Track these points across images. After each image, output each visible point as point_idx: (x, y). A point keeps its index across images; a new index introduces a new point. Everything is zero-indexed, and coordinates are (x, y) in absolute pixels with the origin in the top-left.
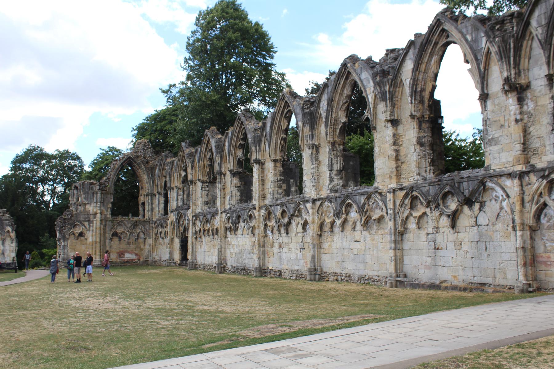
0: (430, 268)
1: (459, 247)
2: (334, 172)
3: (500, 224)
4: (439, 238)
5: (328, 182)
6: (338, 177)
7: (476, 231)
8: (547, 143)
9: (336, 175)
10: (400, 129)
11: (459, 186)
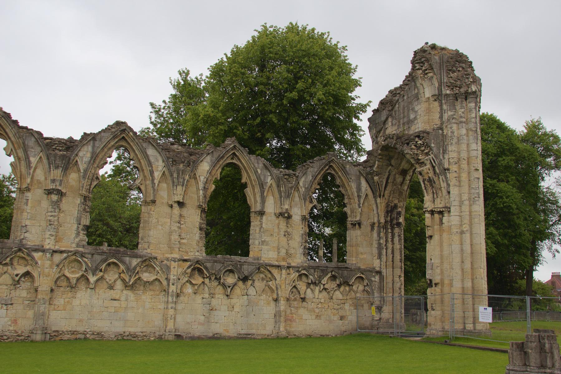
0: (202, 324)
1: (231, 309)
2: (81, 227)
3: (264, 296)
4: (214, 302)
5: (74, 235)
6: (85, 232)
7: (246, 299)
8: (298, 252)
9: (83, 230)
10: (185, 211)
11: (241, 267)
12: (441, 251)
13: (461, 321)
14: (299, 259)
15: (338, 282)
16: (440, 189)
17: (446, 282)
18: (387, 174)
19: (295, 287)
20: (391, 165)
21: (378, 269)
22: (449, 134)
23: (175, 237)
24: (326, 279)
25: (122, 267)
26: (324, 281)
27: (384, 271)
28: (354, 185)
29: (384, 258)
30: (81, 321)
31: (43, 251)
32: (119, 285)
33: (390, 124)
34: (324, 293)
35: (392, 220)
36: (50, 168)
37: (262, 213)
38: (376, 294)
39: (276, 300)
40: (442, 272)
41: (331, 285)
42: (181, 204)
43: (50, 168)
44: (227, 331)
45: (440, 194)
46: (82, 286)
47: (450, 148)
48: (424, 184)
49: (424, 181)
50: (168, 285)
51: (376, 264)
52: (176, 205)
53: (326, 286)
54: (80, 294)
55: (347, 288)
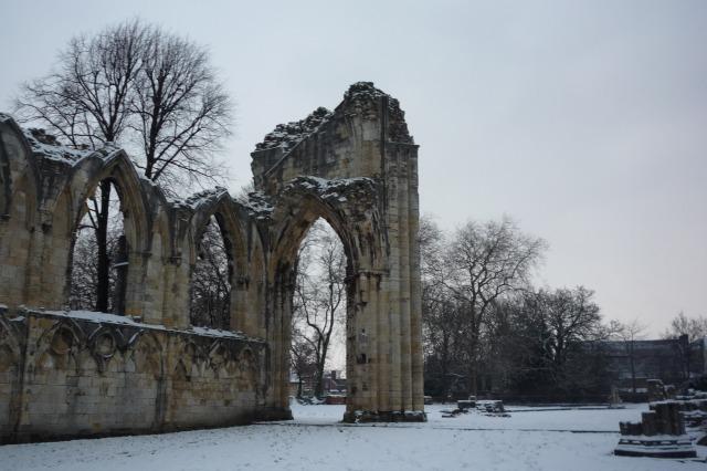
12: (378, 320)
13: (400, 401)
16: (380, 248)
17: (383, 356)
18: (284, 225)
20: (291, 214)
22: (391, 188)
27: (272, 344)
28: (244, 231)
29: (271, 328)
33: (291, 165)
35: (283, 282)
37: (147, 256)
38: (262, 373)
39: (160, 380)
40: (379, 348)
44: (97, 425)
45: (378, 254)
47: (391, 203)
48: (360, 240)
49: (360, 237)
50: (23, 354)
52: (39, 229)
55: (234, 364)
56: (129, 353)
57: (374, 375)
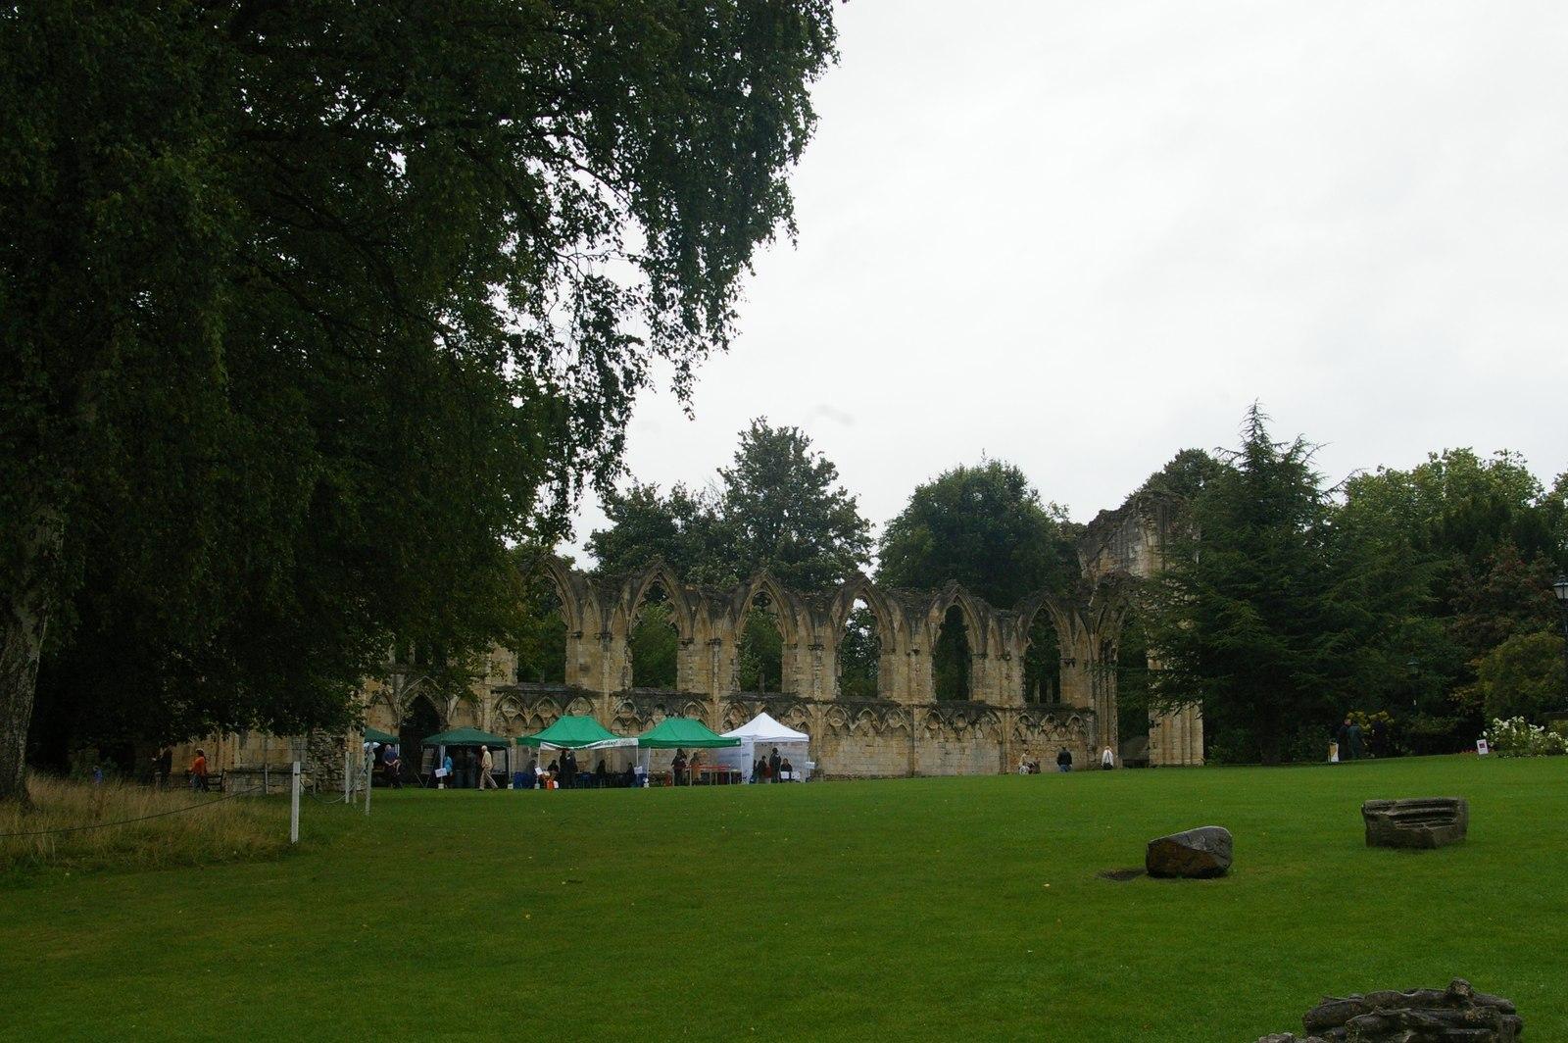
14: (1019, 701)
15: (1055, 723)
19: (1017, 730)
21: (1092, 709)
23: (914, 685)
24: (1044, 721)
25: (875, 716)
26: (1043, 722)
27: (1098, 713)
29: (1098, 698)
30: (845, 765)
31: (816, 703)
32: (871, 732)
34: (1043, 735)
36: (813, 625)
37: (984, 655)
39: (1000, 743)
41: (1048, 727)
42: (916, 652)
43: (813, 625)
46: (843, 732)
50: (913, 729)
51: (1091, 703)
53: (1044, 728)
54: (843, 742)
55: (1063, 729)
56: (978, 726)
57: (1160, 738)
